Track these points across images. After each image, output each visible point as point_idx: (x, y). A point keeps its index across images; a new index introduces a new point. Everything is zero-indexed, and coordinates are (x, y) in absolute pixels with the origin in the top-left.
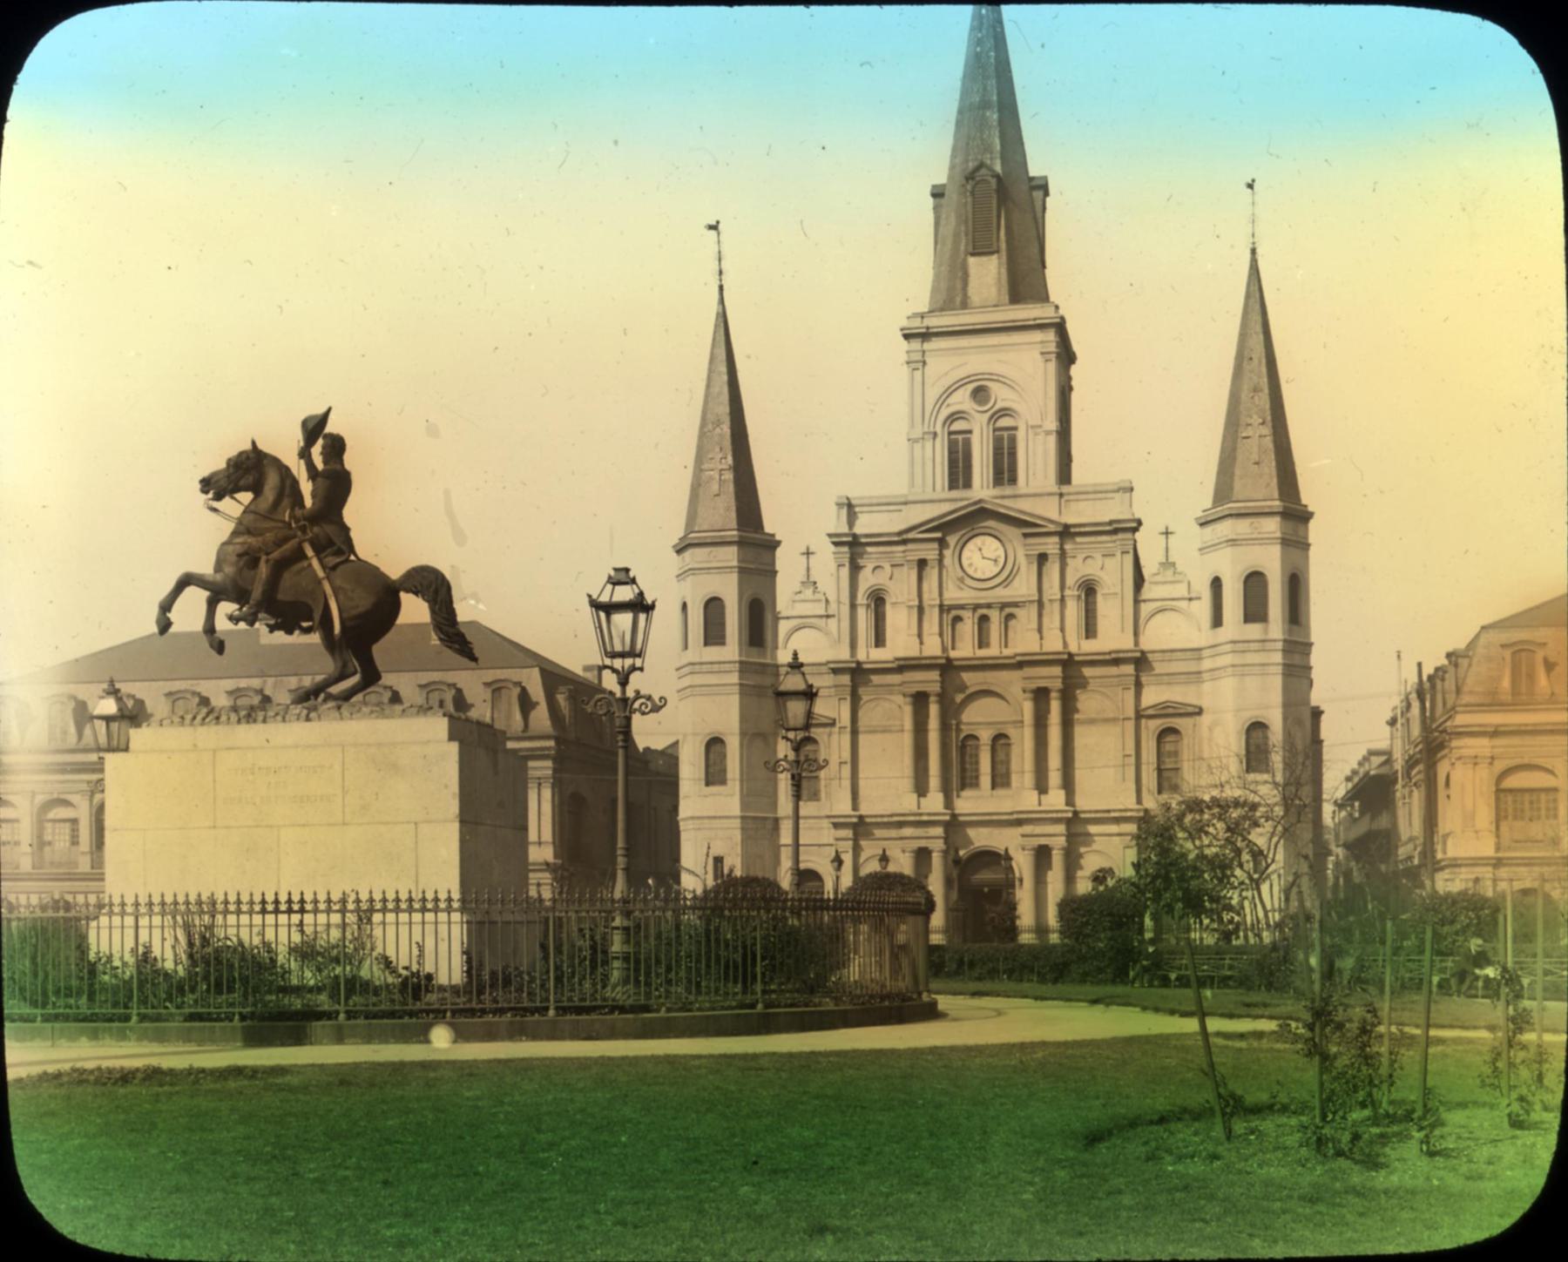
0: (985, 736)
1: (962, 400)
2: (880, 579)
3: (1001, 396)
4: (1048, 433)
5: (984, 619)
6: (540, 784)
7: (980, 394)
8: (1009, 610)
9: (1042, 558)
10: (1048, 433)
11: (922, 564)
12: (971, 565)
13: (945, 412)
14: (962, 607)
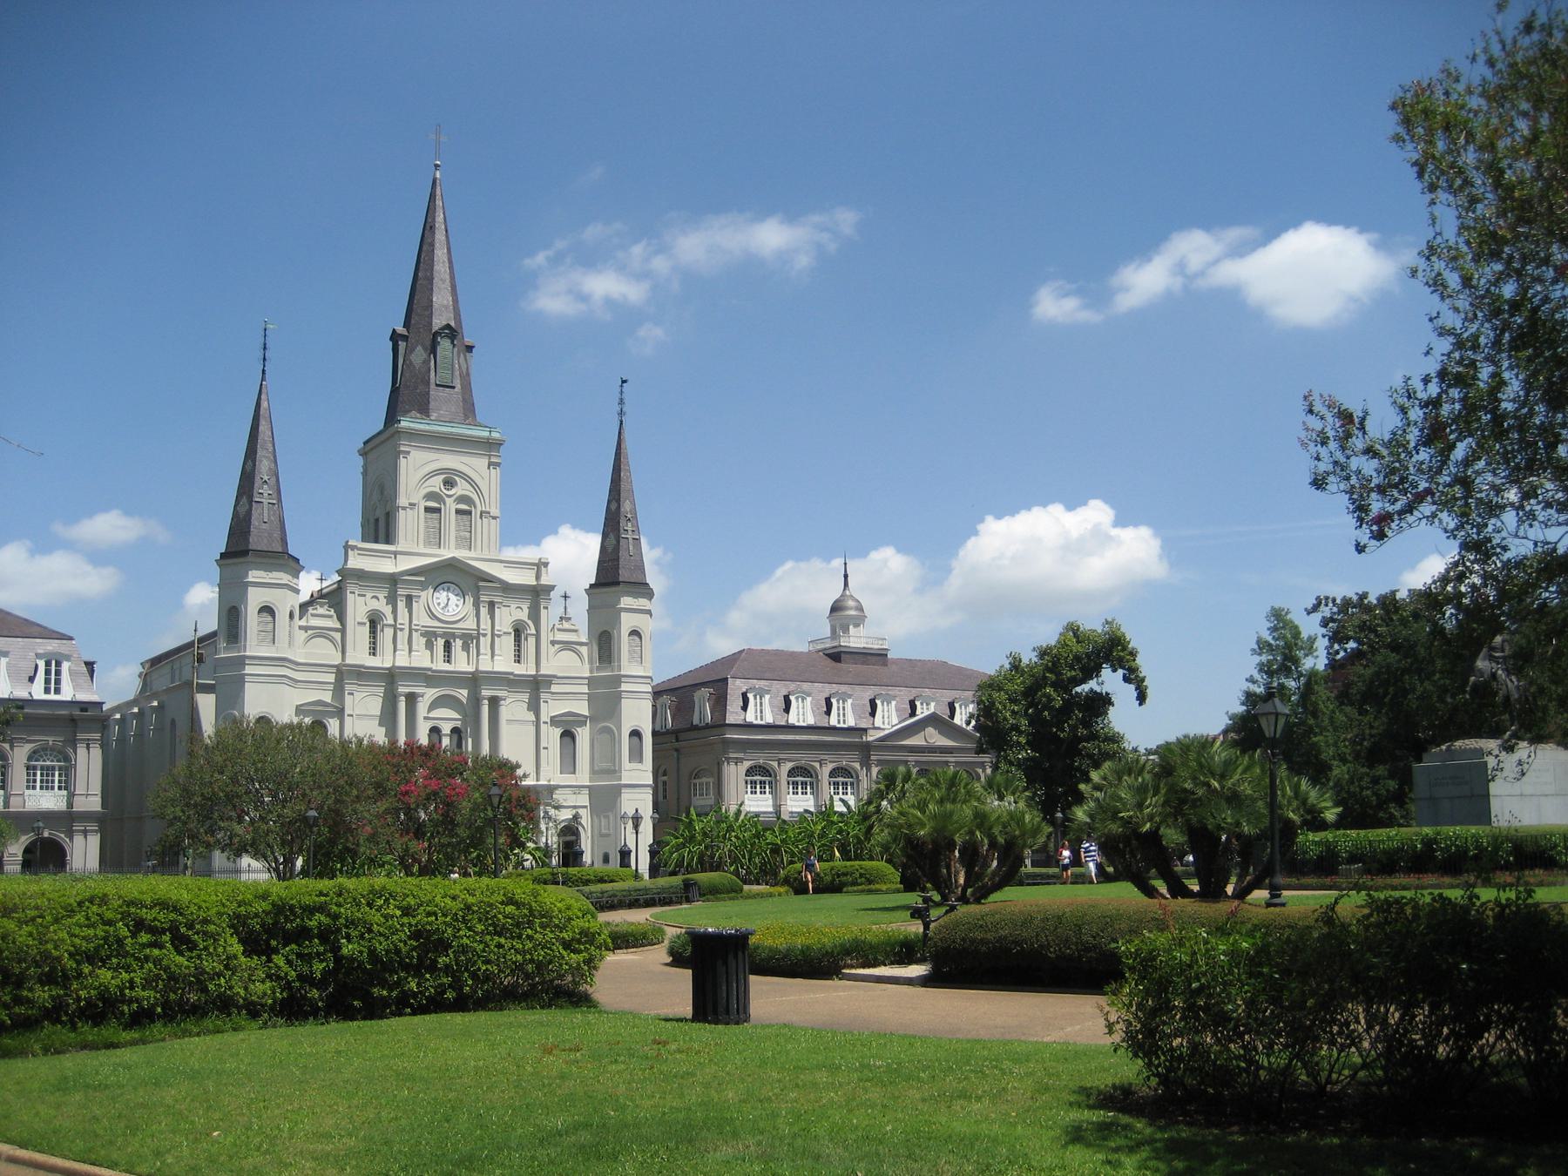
0: (446, 728)
1: (436, 484)
2: (374, 605)
3: (462, 488)
4: (494, 518)
5: (448, 647)
6: (88, 745)
7: (449, 483)
8: (470, 639)
9: (492, 605)
10: (494, 518)
11: (409, 599)
12: (439, 604)
13: (424, 492)
14: (435, 635)
